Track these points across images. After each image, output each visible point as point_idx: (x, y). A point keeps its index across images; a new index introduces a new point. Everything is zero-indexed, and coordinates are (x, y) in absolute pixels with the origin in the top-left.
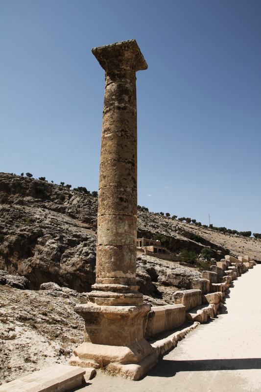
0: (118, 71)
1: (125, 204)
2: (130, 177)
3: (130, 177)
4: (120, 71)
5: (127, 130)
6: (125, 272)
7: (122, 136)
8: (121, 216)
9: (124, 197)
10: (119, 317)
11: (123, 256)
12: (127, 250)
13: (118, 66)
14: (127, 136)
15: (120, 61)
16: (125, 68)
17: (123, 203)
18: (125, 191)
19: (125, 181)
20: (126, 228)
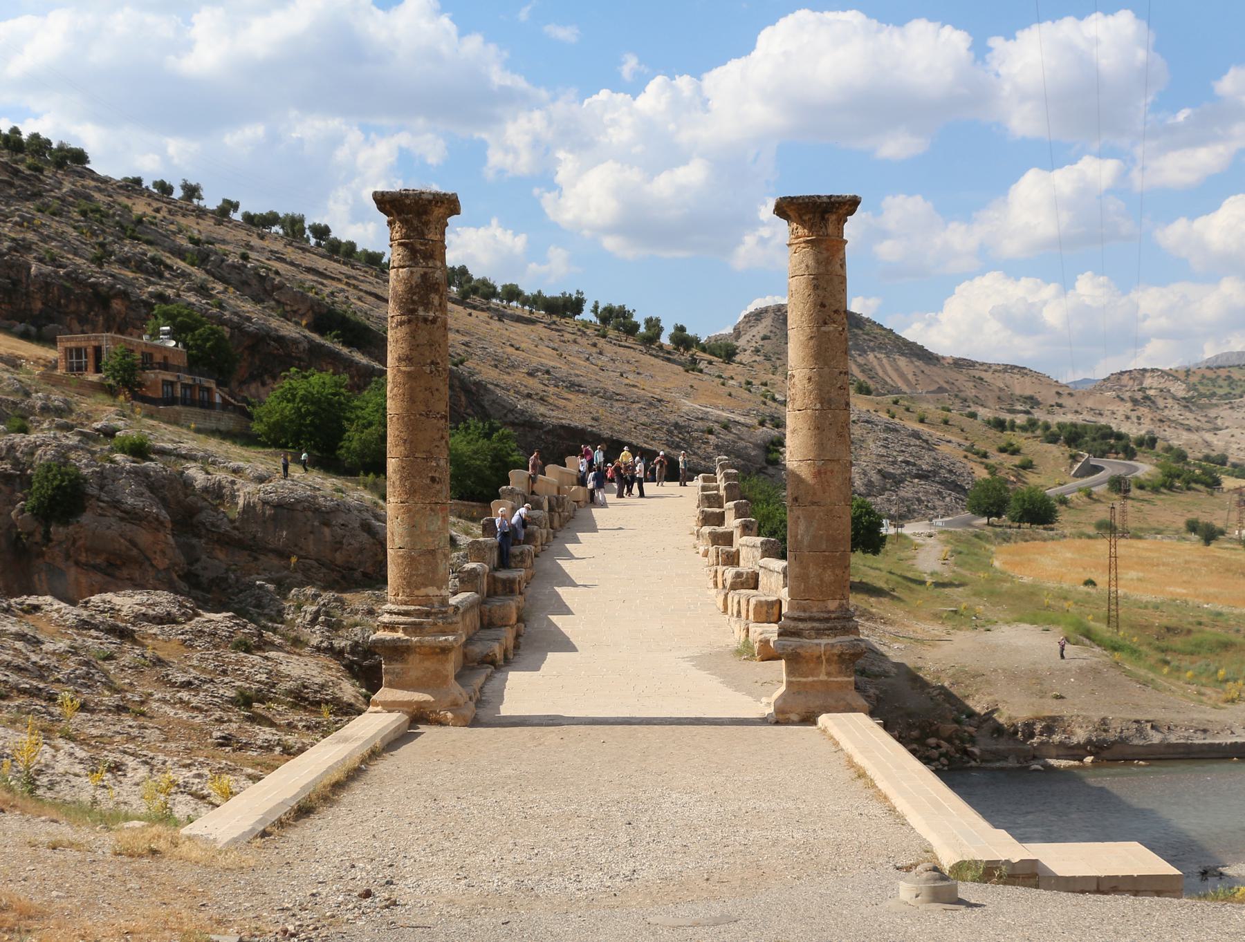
0: (421, 244)
1: (438, 487)
2: (443, 442)
3: (443, 442)
4: (426, 245)
5: (439, 361)
6: (440, 588)
7: (431, 372)
8: (433, 506)
9: (437, 475)
10: (438, 650)
11: (437, 565)
12: (442, 556)
13: (422, 235)
14: (438, 371)
15: (426, 224)
16: (434, 238)
17: (435, 485)
18: (438, 465)
19: (437, 450)
20: (439, 523)
